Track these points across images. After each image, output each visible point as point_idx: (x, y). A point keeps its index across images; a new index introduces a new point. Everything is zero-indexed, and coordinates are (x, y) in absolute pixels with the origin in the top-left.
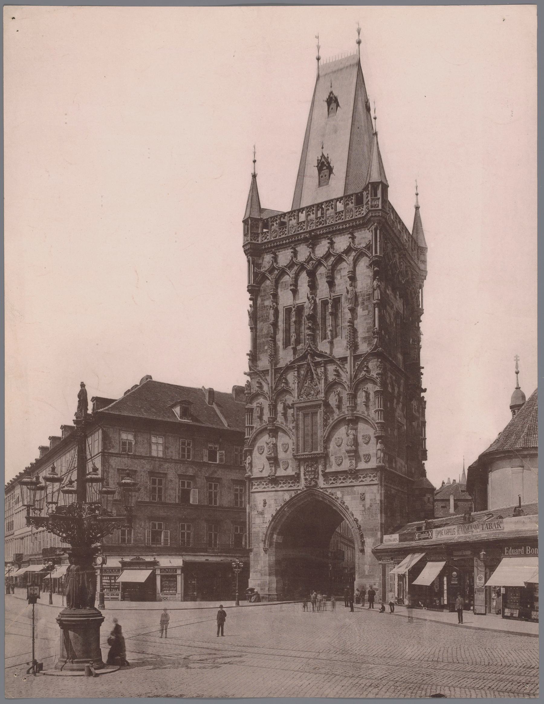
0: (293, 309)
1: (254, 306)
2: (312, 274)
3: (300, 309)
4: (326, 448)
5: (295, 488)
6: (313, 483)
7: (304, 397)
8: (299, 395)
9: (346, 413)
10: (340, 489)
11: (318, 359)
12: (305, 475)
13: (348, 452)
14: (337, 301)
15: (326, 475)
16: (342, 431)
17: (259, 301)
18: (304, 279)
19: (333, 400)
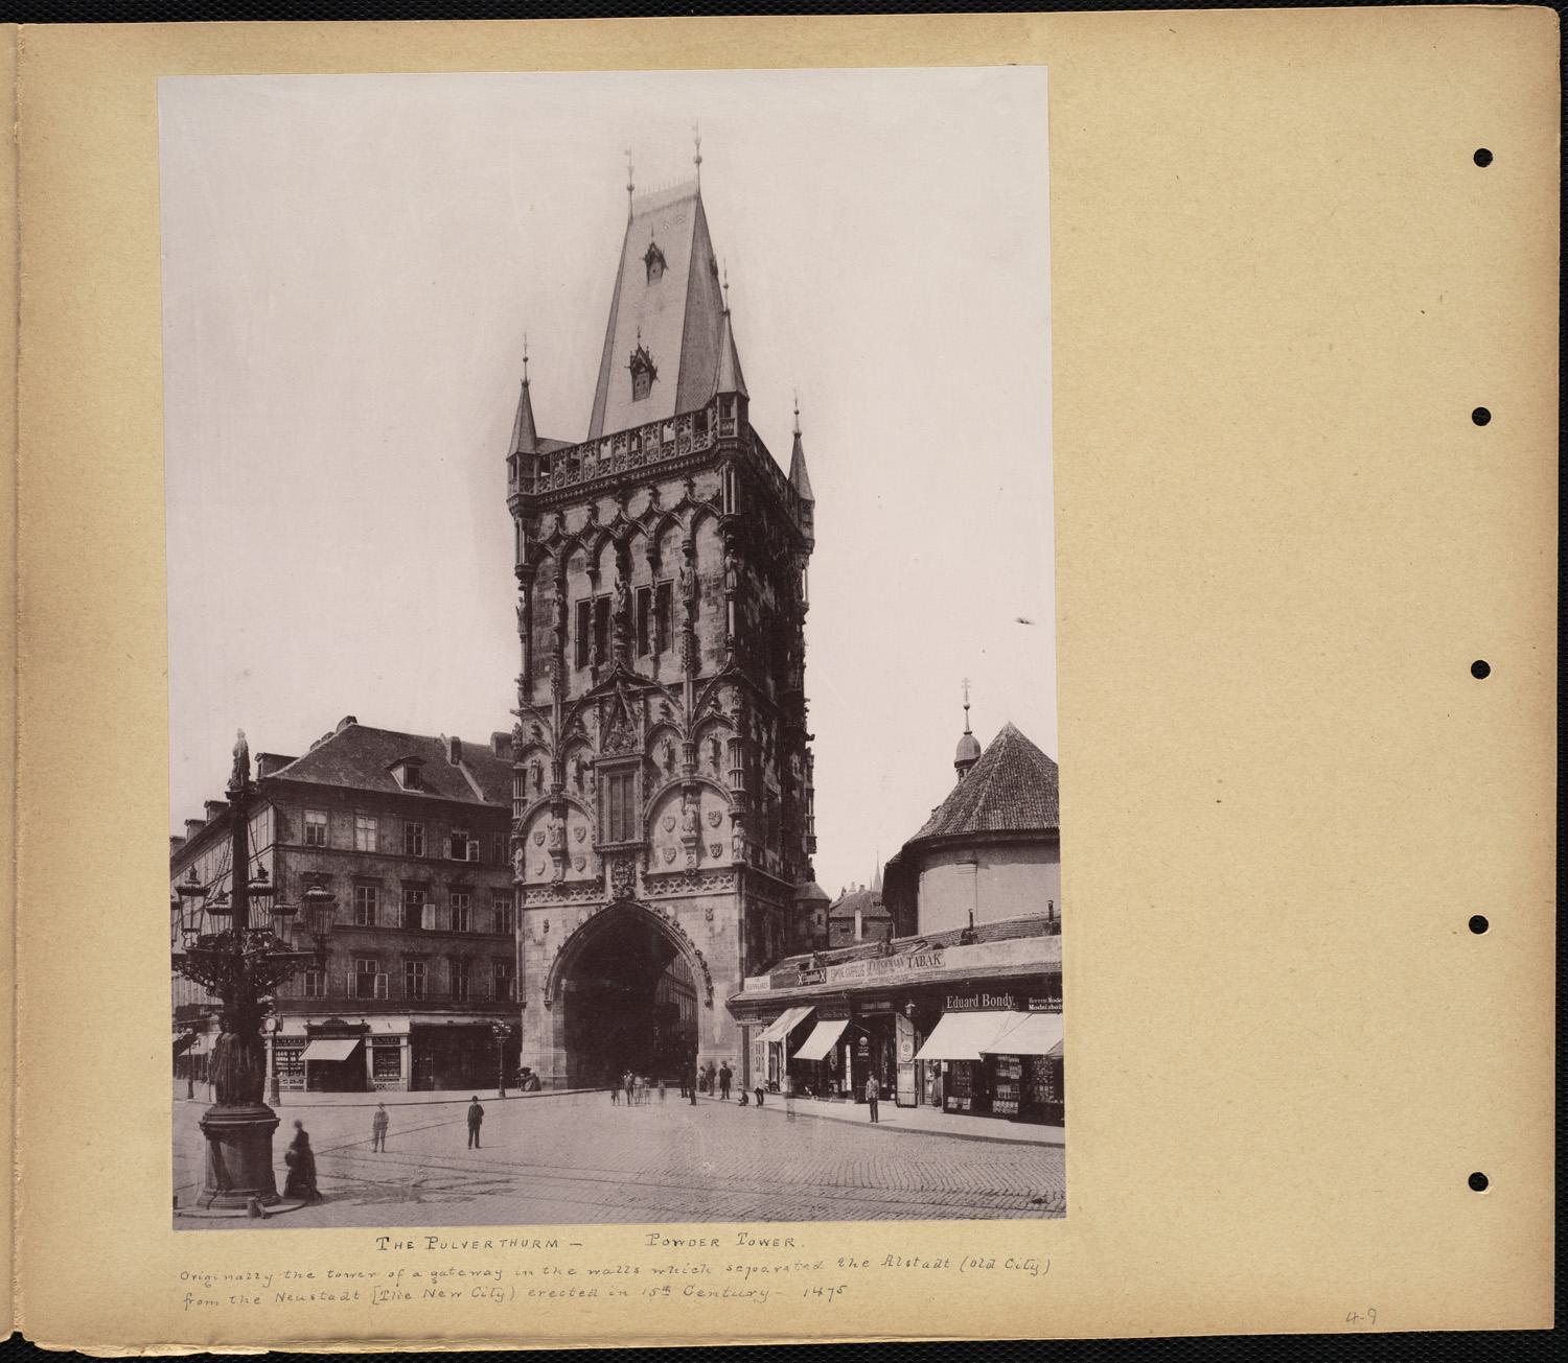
0: (592, 605)
1: (528, 599)
2: (623, 547)
3: (604, 603)
4: (648, 834)
5: (597, 901)
6: (627, 893)
7: (611, 749)
8: (604, 747)
9: (682, 775)
10: (673, 902)
11: (634, 688)
12: (613, 880)
13: (685, 840)
14: (665, 590)
15: (647, 879)
16: (675, 805)
17: (535, 592)
18: (609, 554)
19: (659, 756)
